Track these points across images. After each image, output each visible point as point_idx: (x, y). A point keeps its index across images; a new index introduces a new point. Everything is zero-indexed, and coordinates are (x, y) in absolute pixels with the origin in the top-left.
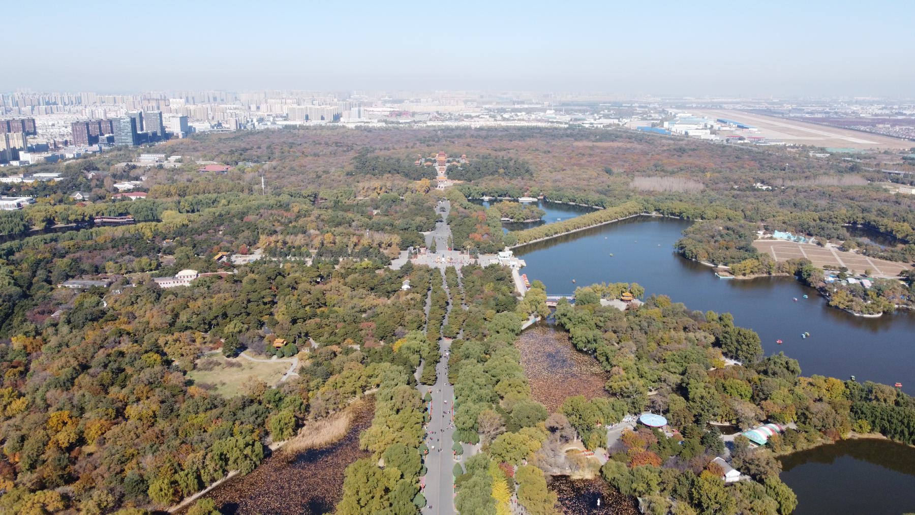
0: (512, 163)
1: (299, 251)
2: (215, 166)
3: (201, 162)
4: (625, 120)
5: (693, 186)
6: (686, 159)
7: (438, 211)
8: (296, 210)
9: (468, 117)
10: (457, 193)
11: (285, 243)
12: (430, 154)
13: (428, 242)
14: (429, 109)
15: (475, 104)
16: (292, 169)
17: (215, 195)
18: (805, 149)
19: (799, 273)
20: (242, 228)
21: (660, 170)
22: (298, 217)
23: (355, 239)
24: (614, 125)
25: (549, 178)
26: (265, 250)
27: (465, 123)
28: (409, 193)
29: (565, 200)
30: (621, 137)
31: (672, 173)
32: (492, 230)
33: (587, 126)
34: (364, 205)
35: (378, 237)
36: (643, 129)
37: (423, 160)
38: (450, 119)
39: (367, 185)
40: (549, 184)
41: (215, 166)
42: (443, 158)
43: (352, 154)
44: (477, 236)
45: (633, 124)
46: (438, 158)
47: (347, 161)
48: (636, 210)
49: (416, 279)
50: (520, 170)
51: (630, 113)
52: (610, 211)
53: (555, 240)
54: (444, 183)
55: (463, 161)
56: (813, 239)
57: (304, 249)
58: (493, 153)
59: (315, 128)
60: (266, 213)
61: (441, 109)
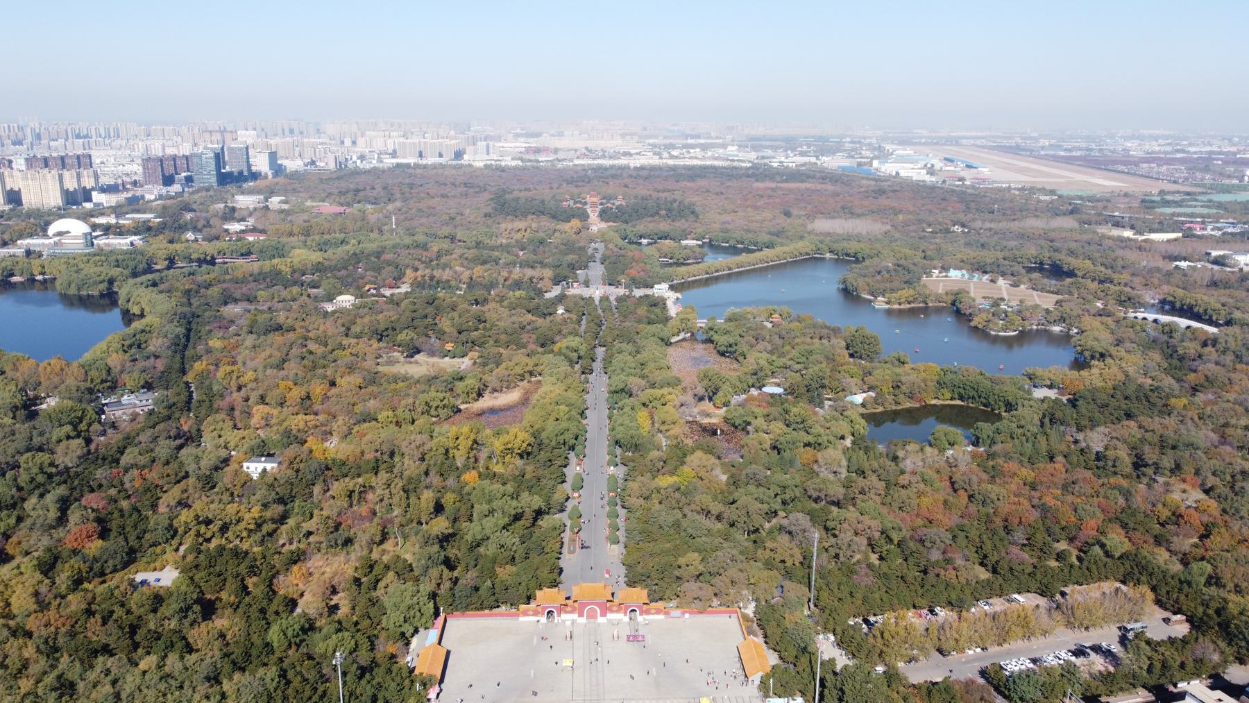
0: (675, 205)
1: (447, 285)
2: (328, 208)
3: (309, 203)
4: (824, 158)
6: (884, 201)
7: (590, 251)
8: (435, 249)
9: (626, 154)
10: (612, 234)
11: (432, 278)
12: (579, 195)
13: (582, 277)
14: (574, 144)
15: (636, 138)
16: (419, 210)
17: (343, 236)
18: (1033, 190)
19: (953, 304)
20: (381, 265)
21: (849, 212)
22: (439, 256)
23: (505, 274)
24: (810, 163)
25: (717, 217)
26: (412, 284)
27: (623, 161)
28: (557, 234)
29: (732, 242)
30: (814, 177)
31: (859, 216)
32: (648, 267)
33: (775, 165)
34: (508, 245)
35: (529, 272)
36: (844, 168)
37: (571, 203)
38: (603, 157)
39: (510, 226)
40: (717, 226)
41: (328, 208)
42: (595, 199)
43: (486, 196)
44: (633, 272)
45: (832, 162)
46: (588, 199)
47: (483, 202)
48: (808, 250)
49: (571, 304)
50: (687, 211)
51: (832, 151)
52: (778, 250)
53: (717, 279)
54: (596, 225)
55: (617, 203)
56: (987, 277)
57: (453, 283)
58: (655, 195)
59: (434, 167)
60: (405, 252)
61: (592, 144)
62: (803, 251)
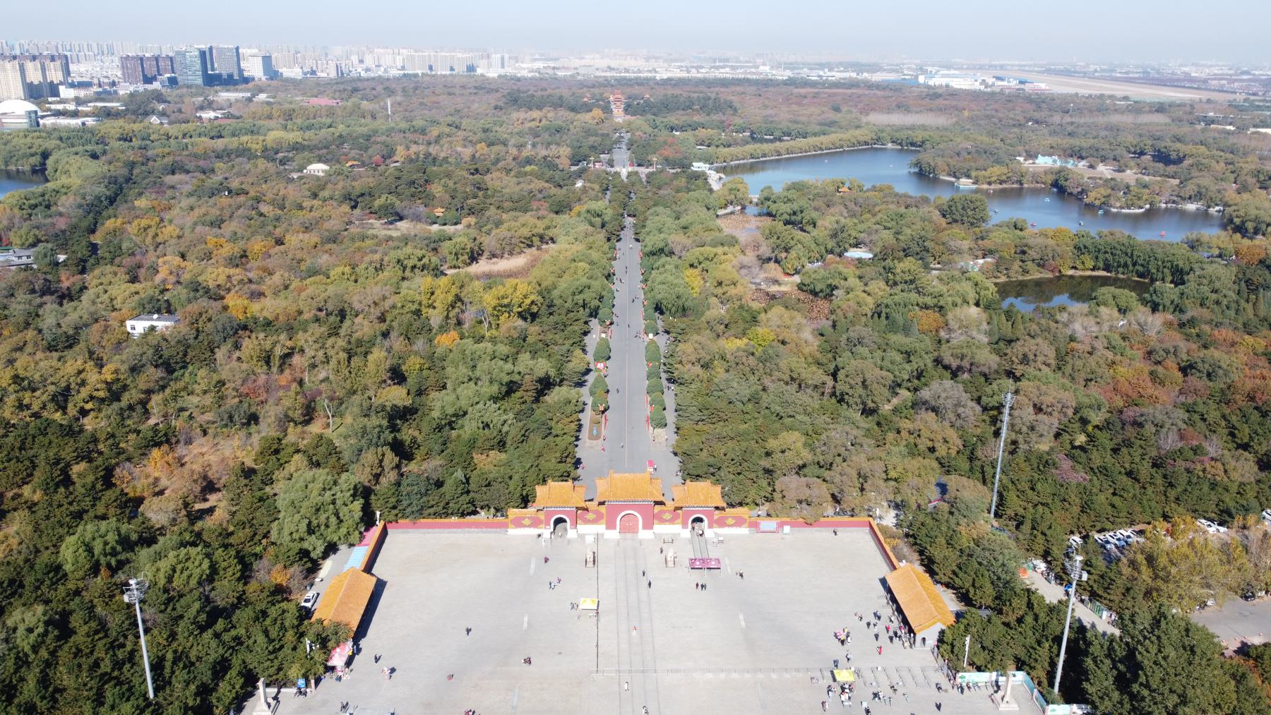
5: (941, 121)
17: (329, 121)
48: (867, 139)
54: (619, 116)
62: (862, 139)
